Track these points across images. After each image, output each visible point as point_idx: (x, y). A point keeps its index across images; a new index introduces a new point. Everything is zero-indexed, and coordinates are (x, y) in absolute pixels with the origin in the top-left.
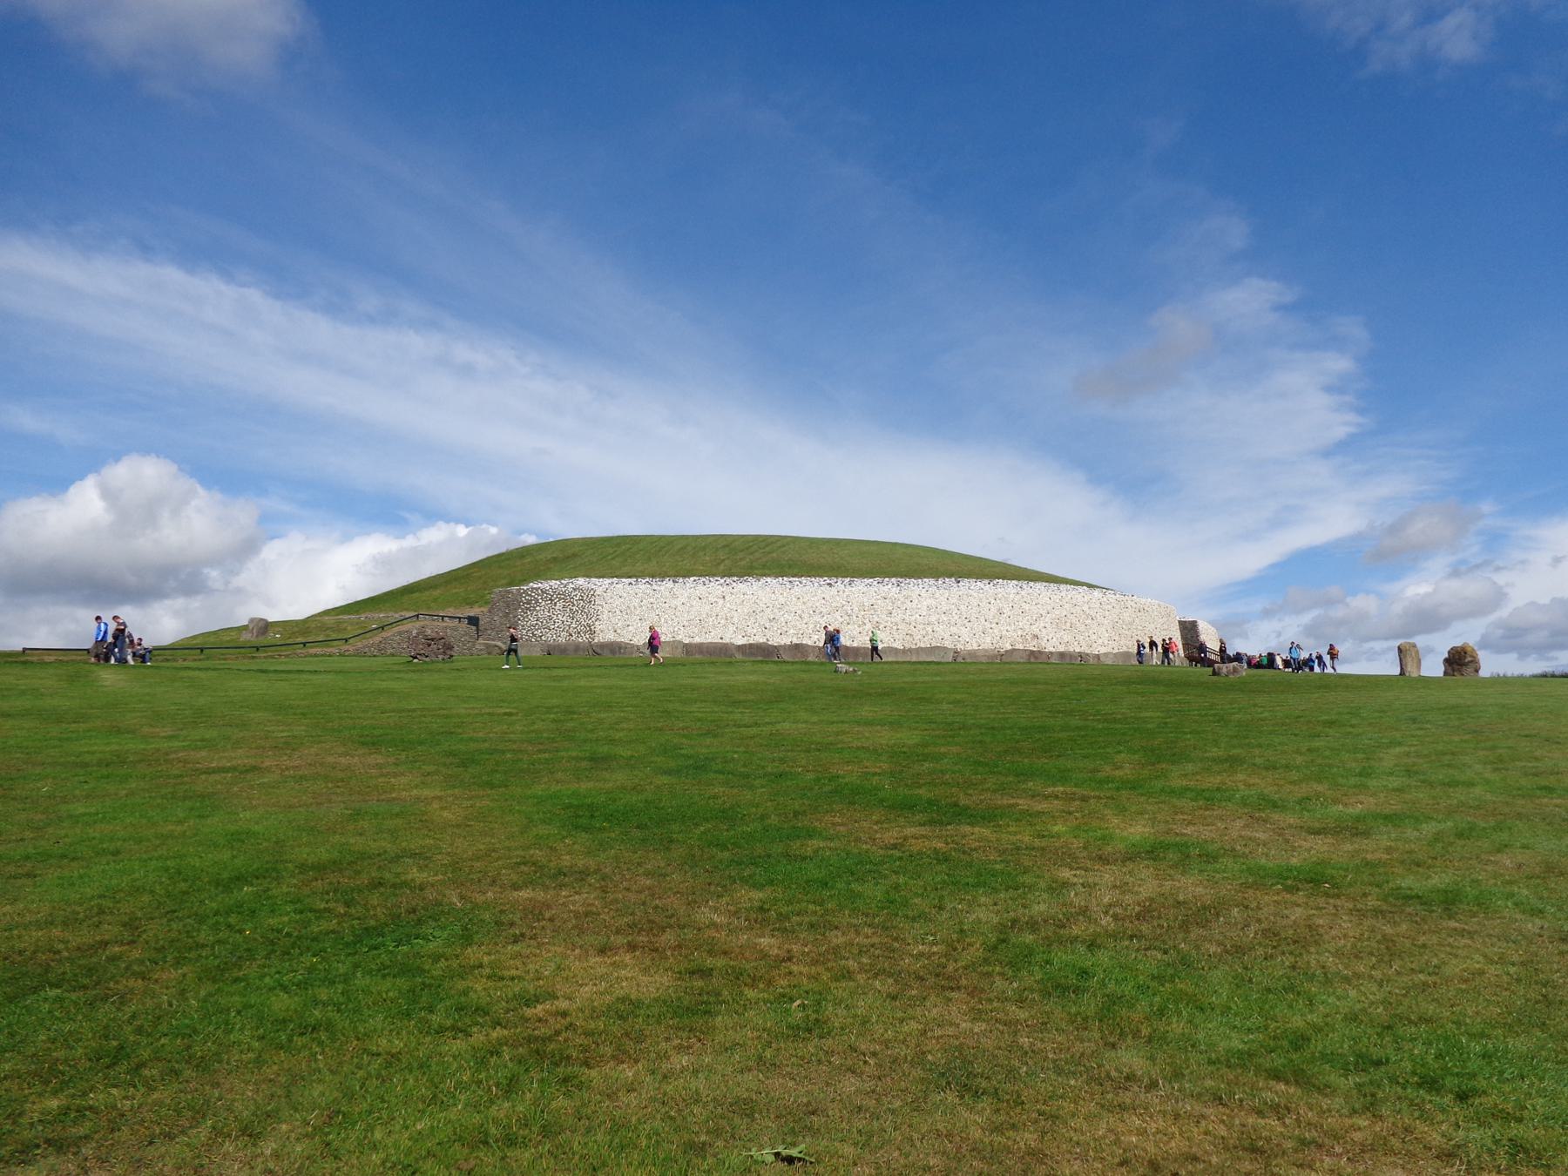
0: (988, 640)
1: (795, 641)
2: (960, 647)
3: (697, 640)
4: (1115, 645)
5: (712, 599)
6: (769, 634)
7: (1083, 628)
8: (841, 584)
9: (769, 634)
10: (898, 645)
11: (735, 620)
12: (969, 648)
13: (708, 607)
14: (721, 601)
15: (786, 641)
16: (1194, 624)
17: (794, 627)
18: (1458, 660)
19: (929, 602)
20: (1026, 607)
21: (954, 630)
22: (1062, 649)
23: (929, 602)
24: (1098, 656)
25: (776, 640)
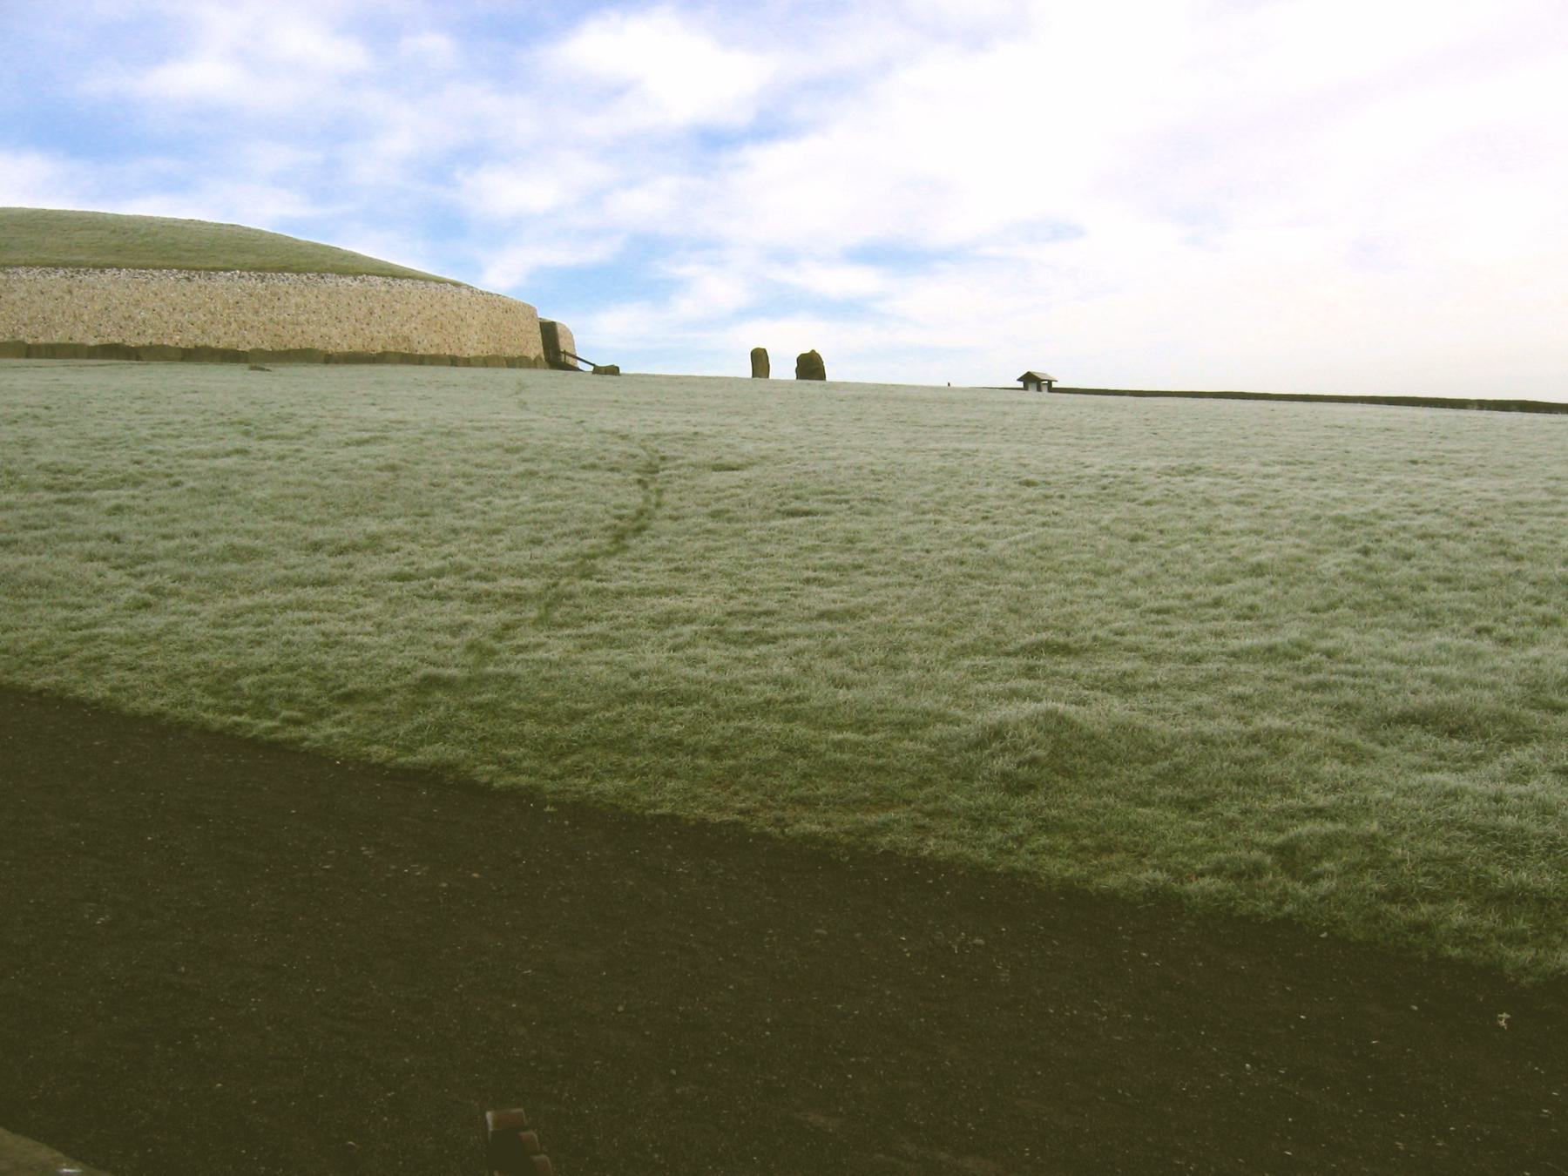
0: (359, 341)
1: (155, 341)
2: (331, 349)
3: (42, 340)
4: (484, 348)
5: (56, 293)
6: (126, 334)
7: (452, 330)
8: (200, 281)
9: (126, 334)
10: (266, 346)
11: (86, 317)
12: (339, 349)
13: (52, 304)
14: (67, 297)
15: (145, 341)
16: (553, 324)
17: (152, 326)
18: (810, 367)
19: (300, 300)
20: (398, 307)
21: (324, 330)
22: (433, 352)
23: (300, 300)
24: (468, 362)
25: (133, 341)
